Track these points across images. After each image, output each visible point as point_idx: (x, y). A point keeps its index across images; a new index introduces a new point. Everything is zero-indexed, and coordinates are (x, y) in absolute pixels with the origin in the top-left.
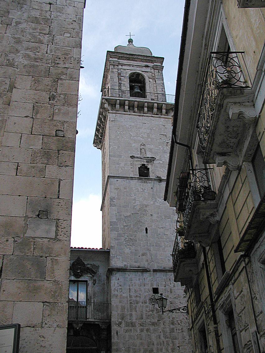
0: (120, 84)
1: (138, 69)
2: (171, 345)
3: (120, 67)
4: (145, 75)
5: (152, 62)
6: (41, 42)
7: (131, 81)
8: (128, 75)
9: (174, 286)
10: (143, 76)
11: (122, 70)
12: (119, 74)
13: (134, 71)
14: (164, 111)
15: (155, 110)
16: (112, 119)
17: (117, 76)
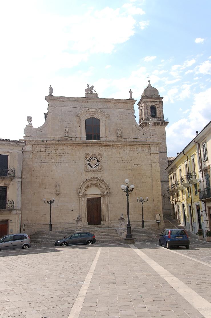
0: (147, 112)
1: (153, 103)
3: (147, 103)
4: (157, 106)
5: (159, 99)
12: (147, 107)
13: (152, 105)
14: (163, 125)
15: (160, 125)
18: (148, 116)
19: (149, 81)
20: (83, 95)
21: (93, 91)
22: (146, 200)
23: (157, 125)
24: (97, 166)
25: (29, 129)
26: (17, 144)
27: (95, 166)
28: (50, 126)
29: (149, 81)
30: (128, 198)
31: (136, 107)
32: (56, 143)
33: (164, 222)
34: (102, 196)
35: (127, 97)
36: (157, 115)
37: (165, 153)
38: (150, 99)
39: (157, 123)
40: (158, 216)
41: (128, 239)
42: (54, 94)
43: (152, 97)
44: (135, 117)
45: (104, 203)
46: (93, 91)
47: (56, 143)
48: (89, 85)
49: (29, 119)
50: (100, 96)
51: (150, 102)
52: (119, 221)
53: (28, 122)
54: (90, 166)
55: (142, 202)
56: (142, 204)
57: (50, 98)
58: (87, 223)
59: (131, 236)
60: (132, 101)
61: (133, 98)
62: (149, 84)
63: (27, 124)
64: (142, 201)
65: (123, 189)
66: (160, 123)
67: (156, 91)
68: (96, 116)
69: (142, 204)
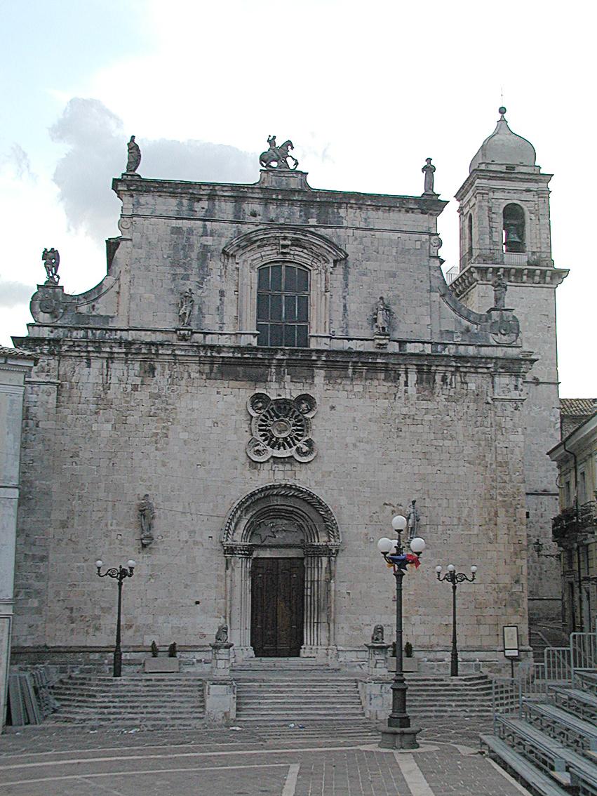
1: (516, 196)
2: (539, 569)
5: (536, 181)
6: (505, 482)
7: (506, 215)
8: (501, 211)
9: (545, 510)
10: (522, 208)
11: (493, 200)
12: (490, 209)
14: (548, 279)
15: (537, 279)
16: (481, 294)
17: (487, 214)
18: (495, 243)
19: (502, 111)
20: (251, 174)
21: (289, 160)
22: (470, 577)
23: (525, 277)
24: (296, 442)
25: (49, 298)
26: (6, 362)
27: (287, 443)
28: (124, 288)
29: (502, 111)
30: (399, 583)
31: (448, 224)
32: (146, 355)
33: (531, 654)
34: (307, 555)
35: (418, 191)
36: (527, 241)
37: (553, 386)
38: (503, 179)
39: (526, 272)
40: (511, 633)
41: (395, 734)
42: (144, 171)
43: (510, 173)
44: (442, 262)
45: (316, 579)
46: (291, 163)
47: (146, 355)
48: (274, 137)
49: (51, 259)
50: (315, 182)
51: (503, 190)
52: (367, 649)
53: (48, 270)
54: (267, 442)
55: (454, 584)
56: (454, 588)
57: (130, 185)
58: (252, 653)
59: (405, 722)
60: (430, 204)
61: (436, 191)
62: (503, 121)
63: (42, 278)
64: (452, 577)
65: (385, 553)
66: (538, 272)
67: (527, 149)
68: (300, 256)
69: (454, 588)
